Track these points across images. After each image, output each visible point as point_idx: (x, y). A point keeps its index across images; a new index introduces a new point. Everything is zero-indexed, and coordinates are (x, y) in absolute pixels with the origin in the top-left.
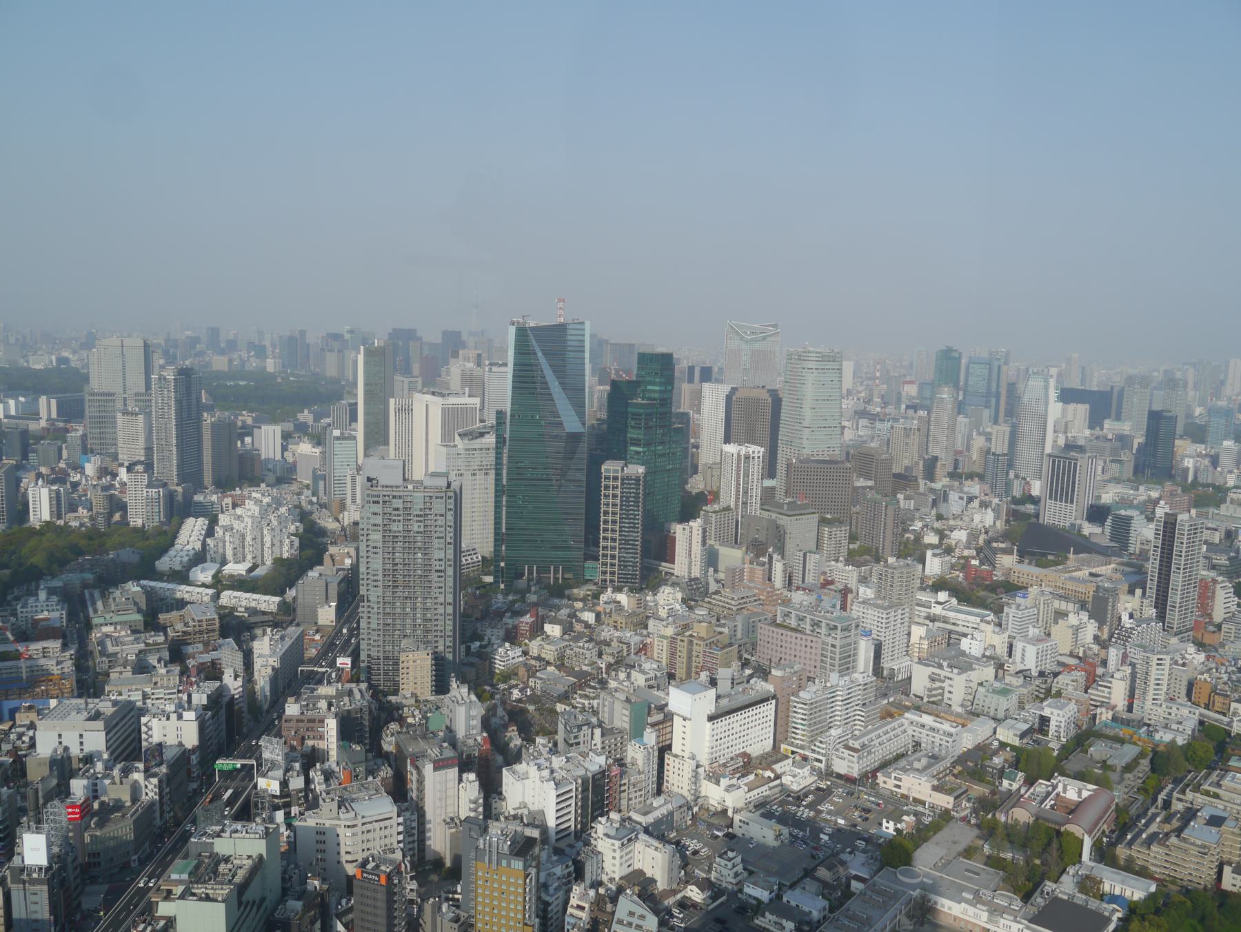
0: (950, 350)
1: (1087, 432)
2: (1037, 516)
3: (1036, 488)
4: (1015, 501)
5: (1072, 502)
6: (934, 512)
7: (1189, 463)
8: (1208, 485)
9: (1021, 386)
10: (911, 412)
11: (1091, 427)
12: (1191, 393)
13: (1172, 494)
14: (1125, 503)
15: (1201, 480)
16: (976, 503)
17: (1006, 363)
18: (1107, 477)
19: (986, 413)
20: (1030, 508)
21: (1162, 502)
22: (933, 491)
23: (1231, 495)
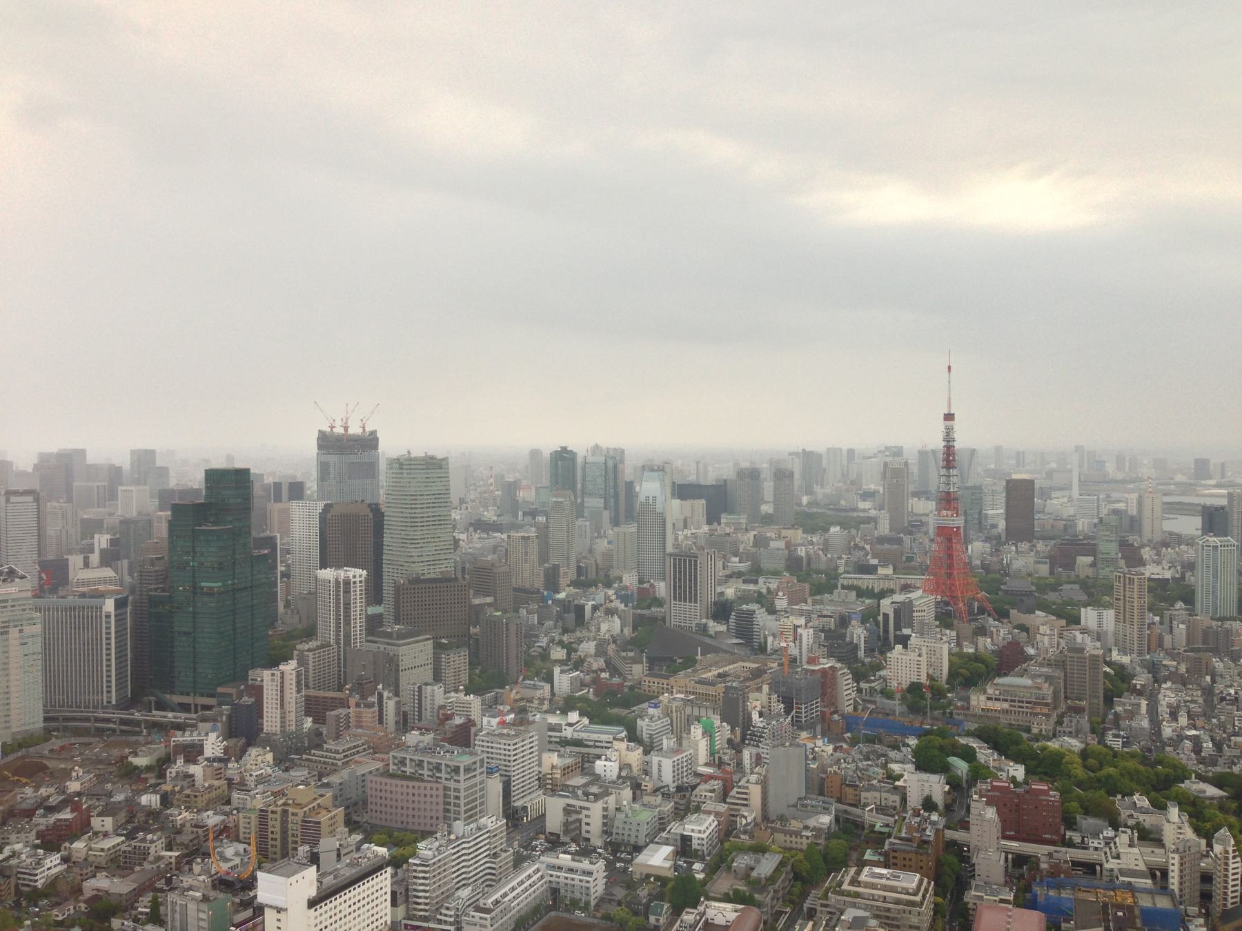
0: (564, 449)
1: (706, 528)
2: (664, 619)
3: (662, 588)
5: (696, 602)
6: (560, 623)
8: (819, 572)
10: (528, 519)
11: (709, 522)
14: (744, 598)
15: (814, 566)
16: (602, 609)
17: (622, 461)
18: (728, 572)
19: (606, 515)
21: (781, 594)
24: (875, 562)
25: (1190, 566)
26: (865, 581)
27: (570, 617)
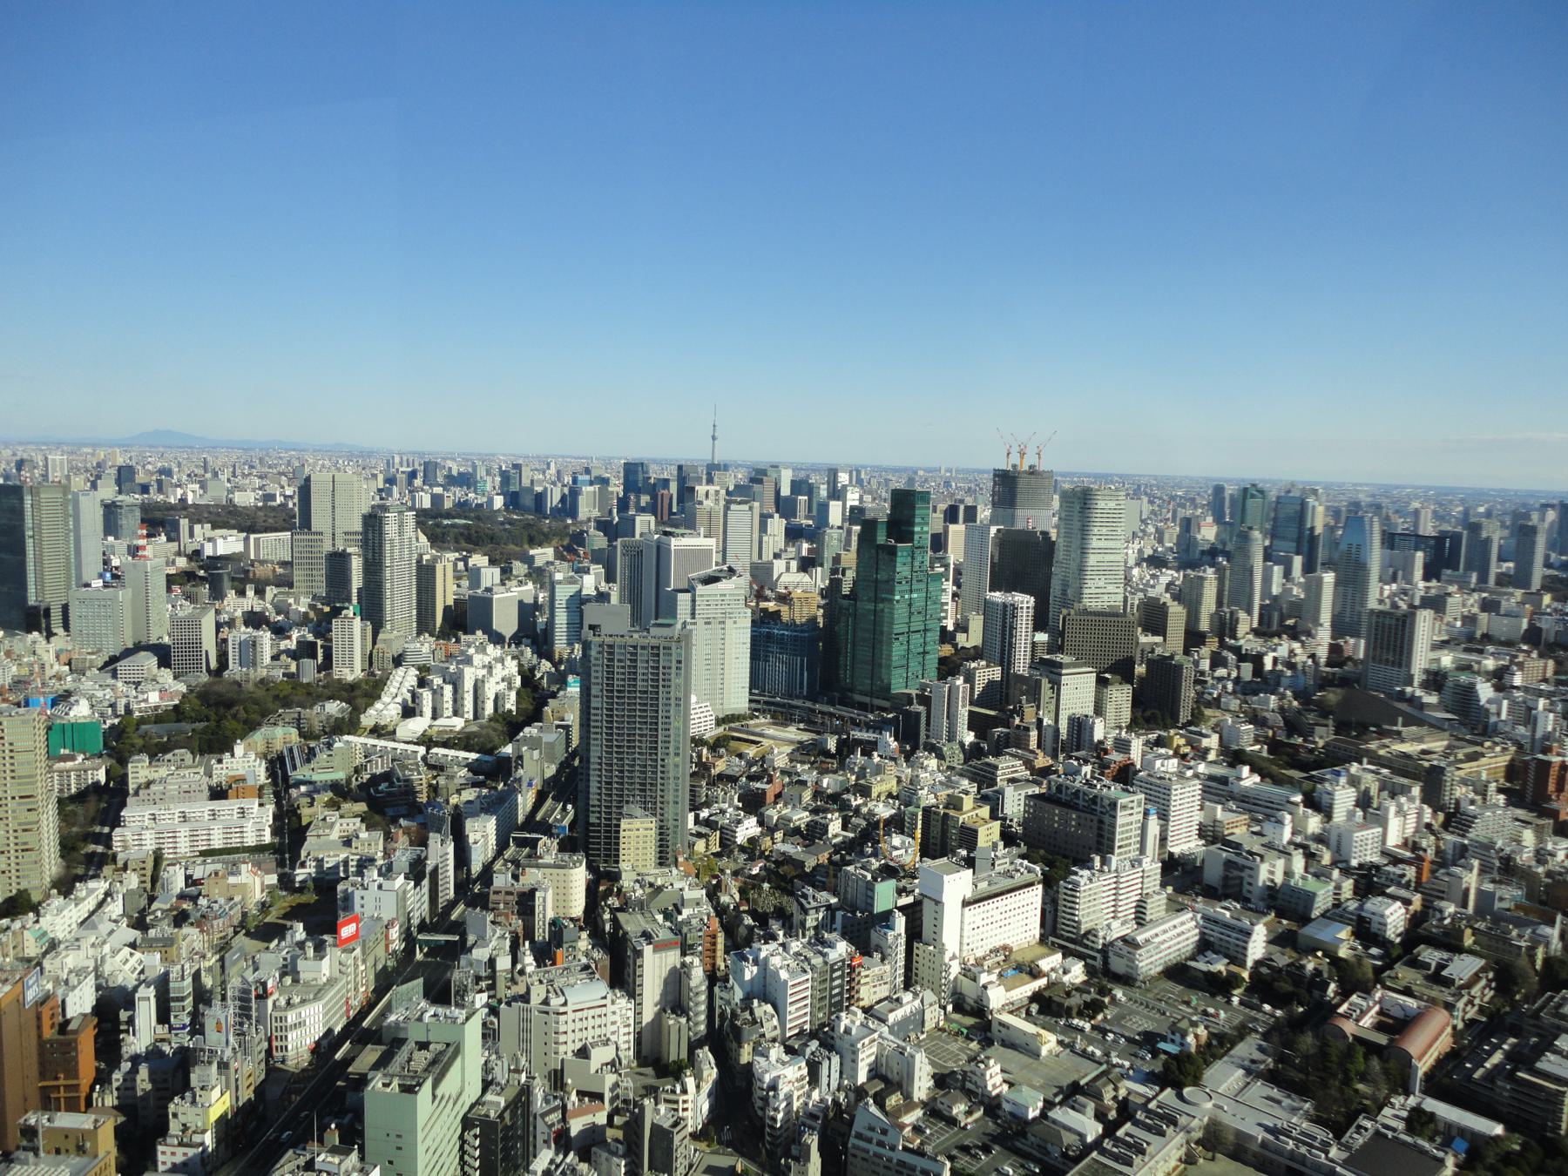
0: (1254, 485)
1: (1421, 584)
3: (1357, 647)
5: (1400, 666)
27: (1247, 668)
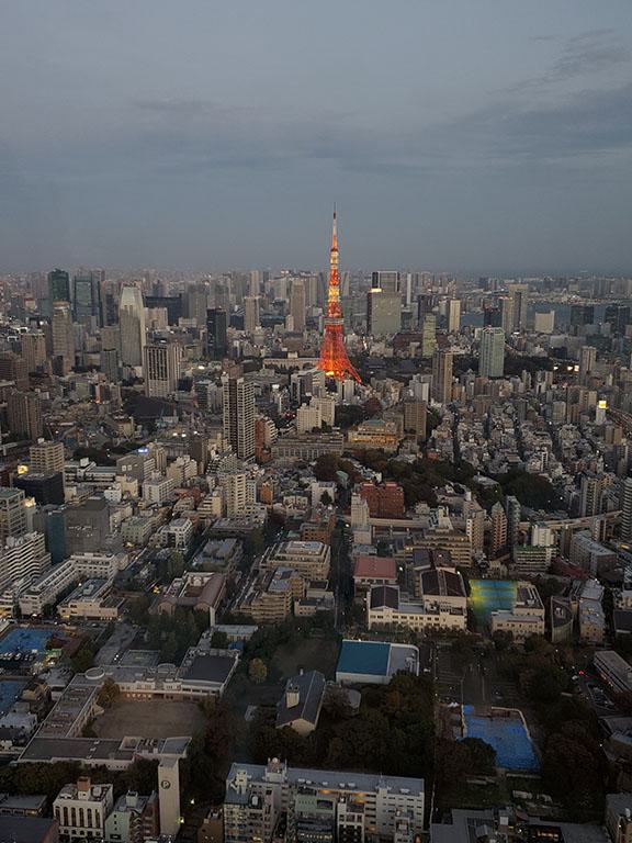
1: (168, 328)
3: (139, 371)
4: (126, 383)
7: (237, 344)
9: (116, 297)
11: (170, 325)
12: (231, 296)
13: (230, 367)
14: (199, 375)
15: (245, 354)
19: (94, 319)
20: (138, 387)
22: (62, 383)
23: (266, 362)
24: (285, 349)
25: (476, 346)
26: (280, 363)
